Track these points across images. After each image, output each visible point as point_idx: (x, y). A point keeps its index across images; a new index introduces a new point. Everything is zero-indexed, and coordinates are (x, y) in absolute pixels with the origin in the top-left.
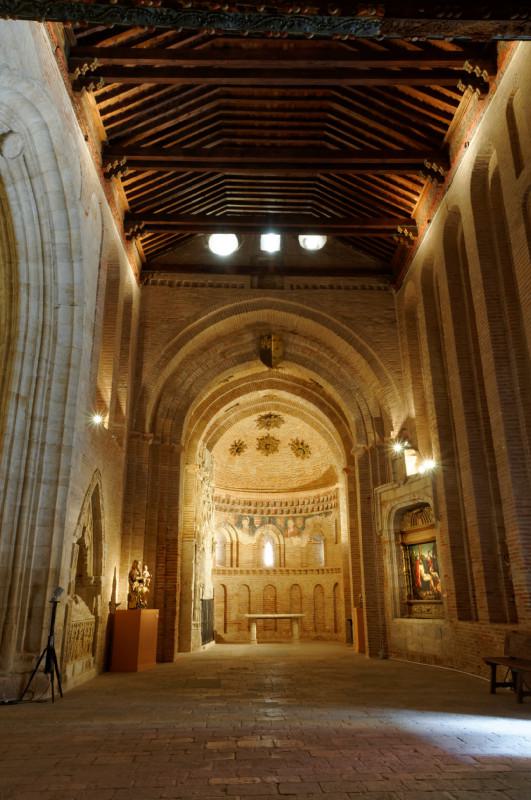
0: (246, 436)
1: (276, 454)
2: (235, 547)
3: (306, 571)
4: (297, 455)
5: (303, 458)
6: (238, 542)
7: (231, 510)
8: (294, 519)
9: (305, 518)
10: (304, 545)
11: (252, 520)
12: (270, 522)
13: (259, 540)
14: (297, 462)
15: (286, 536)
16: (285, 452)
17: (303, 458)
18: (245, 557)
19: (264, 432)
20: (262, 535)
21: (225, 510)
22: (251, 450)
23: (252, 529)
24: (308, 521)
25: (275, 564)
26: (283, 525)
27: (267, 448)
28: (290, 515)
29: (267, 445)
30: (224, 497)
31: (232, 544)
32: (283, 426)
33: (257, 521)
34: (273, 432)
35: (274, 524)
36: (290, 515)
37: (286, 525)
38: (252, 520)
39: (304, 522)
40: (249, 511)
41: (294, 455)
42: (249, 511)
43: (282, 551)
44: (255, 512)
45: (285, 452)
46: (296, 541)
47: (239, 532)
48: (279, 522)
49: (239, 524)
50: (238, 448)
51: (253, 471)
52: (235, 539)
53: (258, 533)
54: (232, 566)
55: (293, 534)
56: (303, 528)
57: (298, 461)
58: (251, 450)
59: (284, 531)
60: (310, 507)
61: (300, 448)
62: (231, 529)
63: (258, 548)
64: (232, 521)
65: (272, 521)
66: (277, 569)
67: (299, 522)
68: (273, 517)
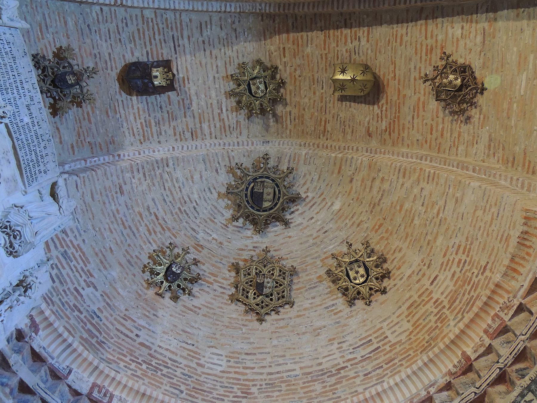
14: (353, 323)
16: (314, 303)
19: (245, 242)
22: (213, 295)
32: (298, 216)
34: (278, 241)
41: (340, 301)
58: (213, 295)
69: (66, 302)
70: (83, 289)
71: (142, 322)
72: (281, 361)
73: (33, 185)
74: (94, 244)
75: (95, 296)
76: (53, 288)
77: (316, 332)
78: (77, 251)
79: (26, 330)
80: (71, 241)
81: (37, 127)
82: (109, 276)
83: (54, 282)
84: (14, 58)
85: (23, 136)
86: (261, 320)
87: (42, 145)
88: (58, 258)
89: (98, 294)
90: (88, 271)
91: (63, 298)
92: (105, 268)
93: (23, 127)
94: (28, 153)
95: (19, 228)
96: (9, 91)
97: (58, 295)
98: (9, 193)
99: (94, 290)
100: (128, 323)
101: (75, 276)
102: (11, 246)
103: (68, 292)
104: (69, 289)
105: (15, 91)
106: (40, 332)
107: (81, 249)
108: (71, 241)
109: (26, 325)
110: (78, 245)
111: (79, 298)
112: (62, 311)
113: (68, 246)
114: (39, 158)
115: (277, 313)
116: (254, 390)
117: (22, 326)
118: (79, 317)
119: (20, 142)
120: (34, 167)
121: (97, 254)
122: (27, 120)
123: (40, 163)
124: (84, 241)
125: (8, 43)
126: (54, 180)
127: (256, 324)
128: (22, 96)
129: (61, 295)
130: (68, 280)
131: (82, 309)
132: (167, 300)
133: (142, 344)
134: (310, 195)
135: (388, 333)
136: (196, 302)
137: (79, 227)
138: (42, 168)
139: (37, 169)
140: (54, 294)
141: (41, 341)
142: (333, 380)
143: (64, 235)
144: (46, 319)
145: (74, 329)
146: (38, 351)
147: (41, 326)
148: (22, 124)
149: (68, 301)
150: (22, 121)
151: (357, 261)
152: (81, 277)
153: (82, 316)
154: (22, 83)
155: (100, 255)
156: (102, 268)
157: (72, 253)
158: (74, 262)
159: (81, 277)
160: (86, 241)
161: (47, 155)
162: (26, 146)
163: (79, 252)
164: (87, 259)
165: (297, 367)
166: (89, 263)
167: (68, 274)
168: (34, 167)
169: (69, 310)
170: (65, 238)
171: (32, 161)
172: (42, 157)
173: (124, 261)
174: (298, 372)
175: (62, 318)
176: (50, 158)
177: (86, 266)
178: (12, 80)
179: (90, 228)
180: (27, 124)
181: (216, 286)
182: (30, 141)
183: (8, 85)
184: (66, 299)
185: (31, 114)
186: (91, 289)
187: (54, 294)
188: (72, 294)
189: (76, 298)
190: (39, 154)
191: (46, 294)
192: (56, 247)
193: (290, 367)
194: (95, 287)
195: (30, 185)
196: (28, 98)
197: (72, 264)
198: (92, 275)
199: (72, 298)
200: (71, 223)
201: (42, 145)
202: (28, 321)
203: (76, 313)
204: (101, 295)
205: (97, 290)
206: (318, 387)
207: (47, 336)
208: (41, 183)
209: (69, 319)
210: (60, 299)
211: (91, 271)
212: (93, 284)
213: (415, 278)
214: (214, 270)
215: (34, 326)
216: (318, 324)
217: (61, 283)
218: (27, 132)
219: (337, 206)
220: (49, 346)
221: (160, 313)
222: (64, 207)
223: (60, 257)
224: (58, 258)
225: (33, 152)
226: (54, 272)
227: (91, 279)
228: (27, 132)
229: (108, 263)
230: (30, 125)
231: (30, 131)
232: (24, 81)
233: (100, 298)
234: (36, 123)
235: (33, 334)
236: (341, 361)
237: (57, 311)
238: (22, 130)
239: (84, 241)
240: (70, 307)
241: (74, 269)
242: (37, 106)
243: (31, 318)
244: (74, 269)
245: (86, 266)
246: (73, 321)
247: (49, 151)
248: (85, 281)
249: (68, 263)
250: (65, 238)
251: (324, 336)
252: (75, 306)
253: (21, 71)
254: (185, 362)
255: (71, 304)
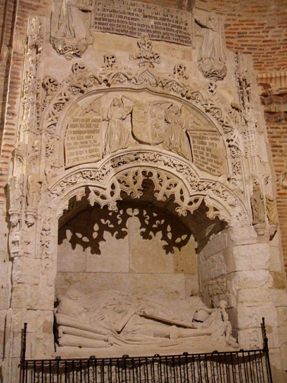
69: (267, 53)
70: (267, 36)
73: (191, 39)
74: (245, 9)
75: (277, 32)
76: (253, 56)
78: (243, 25)
79: (264, 91)
80: (235, 25)
81: (158, 16)
82: (272, 13)
83: (251, 53)
84: (114, 11)
85: (162, 31)
87: (170, 17)
88: (239, 41)
89: (277, 29)
90: (259, 24)
91: (263, 53)
92: (265, 11)
93: (157, 28)
94: (172, 32)
95: (213, 71)
96: (134, 26)
97: (259, 56)
98: (191, 60)
99: (273, 30)
101: (256, 37)
102: (219, 77)
103: (262, 48)
104: (261, 46)
105: (135, 22)
106: (271, 85)
107: (243, 21)
108: (235, 25)
109: (262, 89)
110: (240, 21)
111: (270, 43)
112: (270, 60)
113: (236, 29)
114: (177, 25)
117: (261, 92)
118: (280, 52)
119: (165, 36)
120: (181, 32)
121: (253, 12)
122: (152, 22)
123: (180, 25)
124: (239, 15)
125: (104, 10)
126: (193, 21)
128: (138, 18)
129: (261, 53)
130: (255, 43)
131: (277, 46)
137: (229, 13)
138: (183, 25)
139: (183, 30)
140: (257, 58)
141: (275, 88)
143: (229, 28)
144: (267, 78)
145: (284, 61)
146: (279, 93)
147: (269, 82)
148: (154, 27)
149: (267, 51)
150: (152, 26)
152: (259, 33)
153: (282, 50)
154: (129, 13)
155: (255, 9)
156: (264, 14)
157: (242, 29)
158: (248, 31)
159: (259, 33)
160: (240, 14)
161: (177, 17)
162: (168, 32)
163: (244, 23)
164: (252, 21)
166: (254, 21)
167: (253, 41)
168: (181, 32)
169: (272, 55)
170: (230, 27)
171: (177, 31)
172: (177, 22)
175: (273, 63)
176: (179, 16)
177: (255, 24)
178: (128, 21)
179: (233, 5)
180: (155, 23)
182: (166, 27)
183: (130, 26)
184: (265, 52)
185: (150, 17)
186: (271, 31)
187: (257, 58)
188: (264, 46)
189: (269, 45)
190: (174, 24)
191: (255, 63)
192: (232, 38)
194: (272, 28)
195: (191, 43)
196: (140, 14)
197: (248, 34)
198: (263, 24)
199: (267, 48)
200: (224, 17)
201: (170, 17)
202: (261, 87)
203: (277, 51)
204: (279, 27)
205: (274, 28)
207: (276, 82)
208: (192, 33)
209: (277, 59)
210: (263, 56)
211: (261, 22)
212: (268, 28)
215: (266, 86)
217: (254, 49)
218: (160, 26)
220: (281, 85)
222: (213, 27)
223: (240, 39)
224: (239, 41)
225: (173, 28)
226: (246, 49)
227: (265, 26)
228: (160, 26)
229: (264, 6)
230: (156, 21)
231: (159, 23)
232: (128, 11)
233: (280, 29)
234: (156, 16)
235: (269, 89)
237: (268, 63)
238: (158, 30)
239: (239, 15)
240: (270, 53)
241: (252, 35)
242: (145, 8)
243: (260, 84)
244: (252, 35)
245: (255, 24)
246: (280, 58)
247: (175, 15)
248: (263, 32)
249: (246, 37)
250: (230, 27)
252: (272, 49)
253: (122, 10)
255: (270, 51)
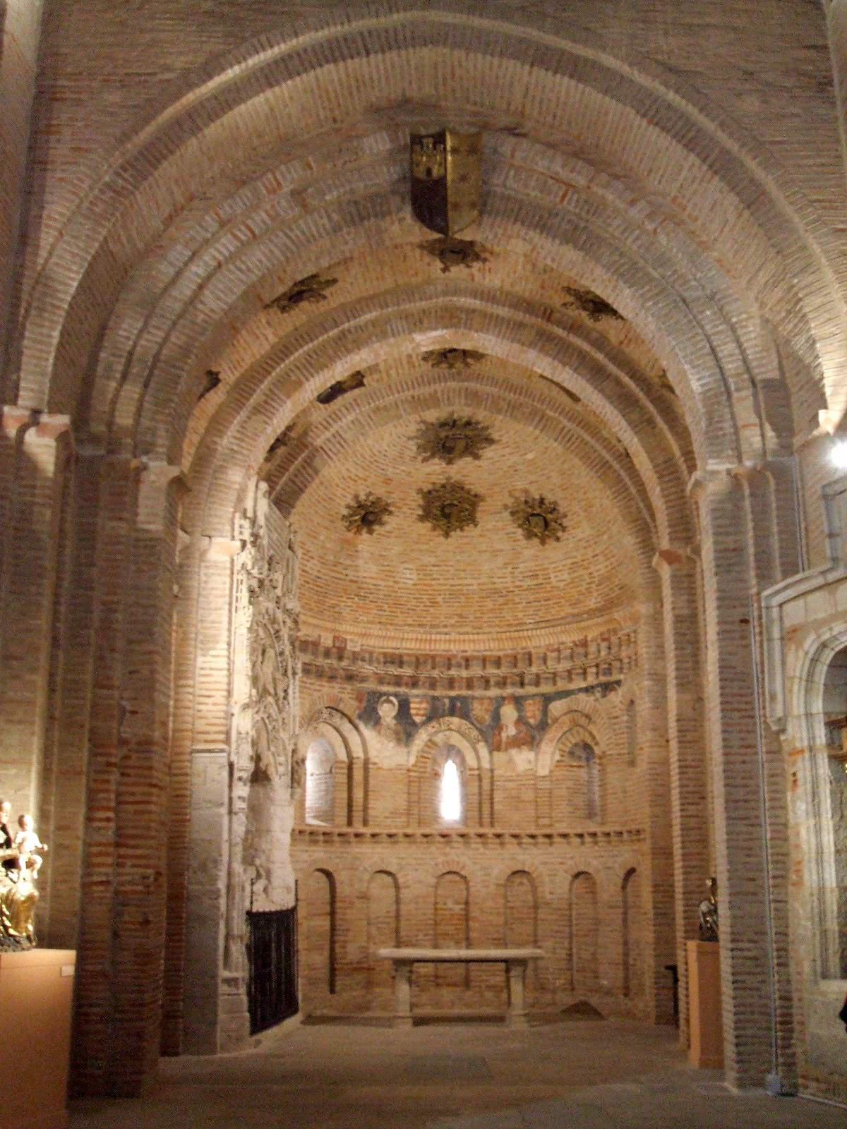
0: (388, 481)
1: (470, 530)
2: (358, 775)
3: (549, 836)
4: (529, 535)
5: (543, 542)
6: (366, 762)
7: (350, 678)
8: (518, 701)
9: (547, 699)
10: (543, 771)
11: (404, 707)
12: (452, 712)
13: (422, 756)
15: (495, 747)
16: (495, 531)
17: (543, 542)
18: (385, 806)
19: (435, 471)
20: (431, 743)
21: (332, 678)
22: (405, 522)
23: (406, 728)
24: (557, 707)
25: (465, 819)
26: (487, 717)
27: (447, 517)
28: (509, 691)
29: (449, 509)
30: (329, 643)
31: (350, 768)
32: (489, 453)
33: (418, 709)
35: (465, 715)
36: (509, 691)
37: (496, 717)
38: (404, 707)
39: (545, 711)
40: (398, 681)
42: (398, 681)
43: (486, 786)
44: (414, 683)
45: (495, 531)
46: (522, 759)
47: (368, 732)
48: (478, 710)
49: (370, 715)
50: (368, 515)
51: (408, 576)
52: (358, 752)
53: (422, 737)
54: (350, 823)
55: (516, 743)
56: (543, 726)
57: (530, 549)
59: (490, 733)
60: (565, 665)
61: (540, 519)
62: (346, 727)
63: (422, 783)
64: (351, 706)
65: (459, 708)
66: (472, 831)
67: (532, 711)
68: (464, 699)
71: (349, 562)
72: (462, 574)
77: (495, 553)
86: (447, 535)
100: (339, 568)
115: (462, 530)
116: (439, 599)
127: (442, 539)
132: (365, 535)
133: (351, 581)
134: (504, 439)
135: (552, 576)
136: (388, 528)
142: (501, 600)
151: (538, 515)
165: (474, 582)
173: (327, 523)
174: (475, 587)
181: (405, 509)
193: (469, 581)
206: (489, 604)
213: (583, 544)
214: (402, 495)
216: (499, 547)
219: (530, 456)
221: (360, 547)
236: (509, 585)
251: (500, 561)
254: (383, 583)
